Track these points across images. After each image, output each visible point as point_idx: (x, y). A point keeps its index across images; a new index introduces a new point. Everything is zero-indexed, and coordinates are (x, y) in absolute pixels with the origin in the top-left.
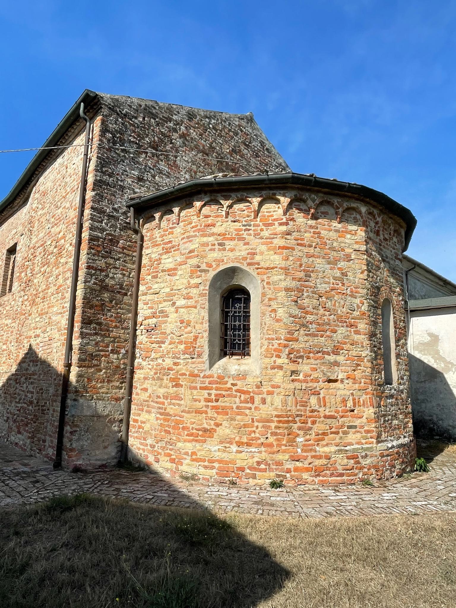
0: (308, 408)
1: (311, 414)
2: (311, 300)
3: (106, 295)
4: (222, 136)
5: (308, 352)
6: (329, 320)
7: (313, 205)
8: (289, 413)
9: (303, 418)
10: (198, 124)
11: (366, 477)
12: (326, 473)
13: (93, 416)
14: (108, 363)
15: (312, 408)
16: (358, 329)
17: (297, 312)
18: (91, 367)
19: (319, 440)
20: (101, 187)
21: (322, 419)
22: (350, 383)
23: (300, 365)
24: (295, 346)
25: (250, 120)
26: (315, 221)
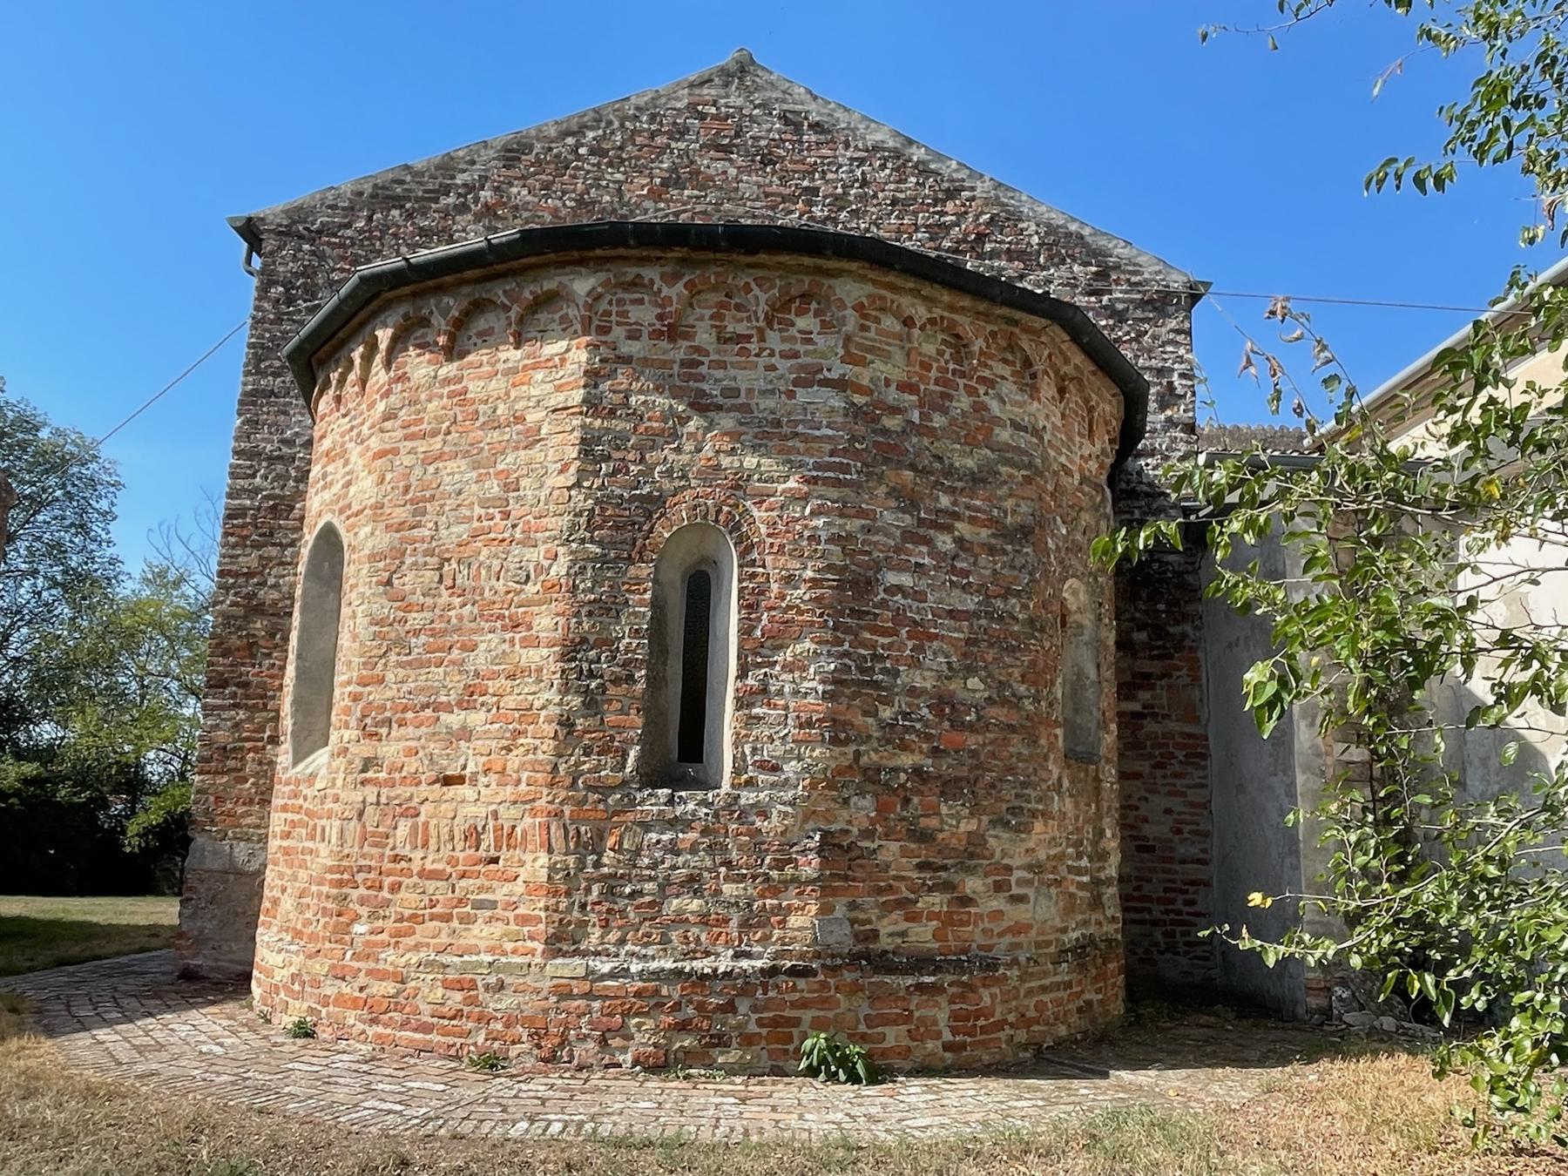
0: (388, 852)
1: (392, 865)
2: (421, 573)
3: (258, 625)
4: (623, 161)
5: (400, 708)
6: (460, 618)
7: (443, 322)
8: (345, 863)
9: (372, 875)
10: (538, 162)
11: (496, 1045)
12: (391, 1018)
13: (226, 873)
14: (260, 763)
15: (397, 851)
16: (533, 632)
17: (386, 611)
18: (223, 773)
19: (398, 934)
20: (254, 404)
21: (415, 879)
22: (493, 786)
23: (384, 742)
24: (376, 695)
25: (742, 71)
26: (456, 364)
